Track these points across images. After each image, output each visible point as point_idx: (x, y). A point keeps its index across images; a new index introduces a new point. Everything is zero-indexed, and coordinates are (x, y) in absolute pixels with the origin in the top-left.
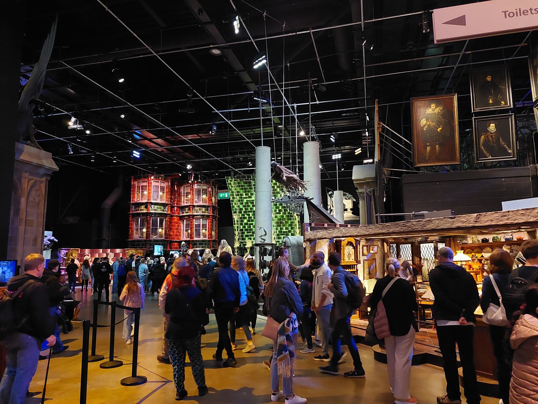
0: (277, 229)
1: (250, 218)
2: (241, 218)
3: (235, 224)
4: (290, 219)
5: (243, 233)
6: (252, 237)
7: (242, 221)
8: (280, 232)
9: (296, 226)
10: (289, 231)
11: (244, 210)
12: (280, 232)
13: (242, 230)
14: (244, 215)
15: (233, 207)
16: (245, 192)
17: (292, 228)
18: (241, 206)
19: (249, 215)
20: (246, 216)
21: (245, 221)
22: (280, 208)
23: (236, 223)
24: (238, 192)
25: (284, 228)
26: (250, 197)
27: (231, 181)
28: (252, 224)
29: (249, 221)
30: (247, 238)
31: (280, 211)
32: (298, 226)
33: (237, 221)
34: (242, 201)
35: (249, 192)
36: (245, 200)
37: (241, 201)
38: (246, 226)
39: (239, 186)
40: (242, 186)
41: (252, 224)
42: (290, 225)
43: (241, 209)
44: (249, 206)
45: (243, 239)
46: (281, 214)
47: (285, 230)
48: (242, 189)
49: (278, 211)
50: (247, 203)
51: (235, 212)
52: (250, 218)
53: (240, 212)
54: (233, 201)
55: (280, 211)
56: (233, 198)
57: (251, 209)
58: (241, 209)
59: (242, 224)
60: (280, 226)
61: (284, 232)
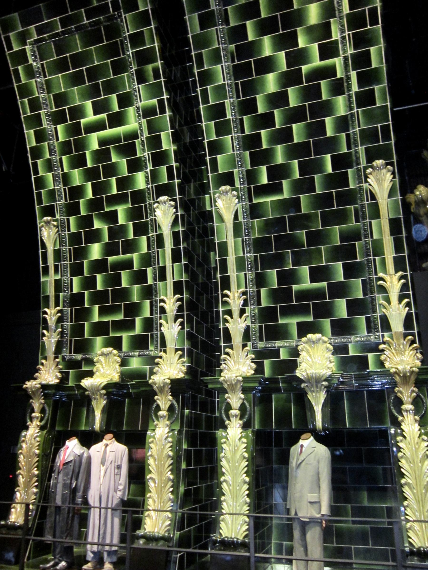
0: (260, 281)
1: (116, 232)
2: (75, 238)
3: (46, 271)
4: (341, 217)
5: (82, 314)
6: (125, 336)
7: (80, 253)
8: (274, 295)
9: (378, 250)
10: (338, 290)
11: (90, 194)
12: (281, 295)
13: (76, 300)
14: (87, 222)
15: (41, 182)
16: (94, 92)
17: (351, 271)
18: (77, 177)
19: (112, 217)
20: (97, 224)
22: (280, 158)
23: (51, 262)
24: (60, 99)
25: (305, 270)
26: (117, 120)
27: (23, 38)
28: (128, 265)
29: (110, 249)
30: (99, 340)
31: (278, 173)
32: (389, 253)
33: (58, 254)
34: (81, 145)
35: (110, 87)
36: (94, 141)
37: (74, 149)
38: (99, 278)
39: (61, 66)
40: (78, 60)
41: (128, 265)
42: (337, 254)
43: (76, 192)
44: (111, 170)
45: (83, 346)
46: (286, 195)
47: (307, 284)
48: (77, 79)
49: (264, 180)
50: (102, 155)
51: (49, 211)
52: (116, 232)
53: (72, 209)
54: (37, 153)
56: (41, 136)
57: (123, 183)
58: (76, 192)
59: (77, 270)
60: (277, 261)
61: (304, 295)
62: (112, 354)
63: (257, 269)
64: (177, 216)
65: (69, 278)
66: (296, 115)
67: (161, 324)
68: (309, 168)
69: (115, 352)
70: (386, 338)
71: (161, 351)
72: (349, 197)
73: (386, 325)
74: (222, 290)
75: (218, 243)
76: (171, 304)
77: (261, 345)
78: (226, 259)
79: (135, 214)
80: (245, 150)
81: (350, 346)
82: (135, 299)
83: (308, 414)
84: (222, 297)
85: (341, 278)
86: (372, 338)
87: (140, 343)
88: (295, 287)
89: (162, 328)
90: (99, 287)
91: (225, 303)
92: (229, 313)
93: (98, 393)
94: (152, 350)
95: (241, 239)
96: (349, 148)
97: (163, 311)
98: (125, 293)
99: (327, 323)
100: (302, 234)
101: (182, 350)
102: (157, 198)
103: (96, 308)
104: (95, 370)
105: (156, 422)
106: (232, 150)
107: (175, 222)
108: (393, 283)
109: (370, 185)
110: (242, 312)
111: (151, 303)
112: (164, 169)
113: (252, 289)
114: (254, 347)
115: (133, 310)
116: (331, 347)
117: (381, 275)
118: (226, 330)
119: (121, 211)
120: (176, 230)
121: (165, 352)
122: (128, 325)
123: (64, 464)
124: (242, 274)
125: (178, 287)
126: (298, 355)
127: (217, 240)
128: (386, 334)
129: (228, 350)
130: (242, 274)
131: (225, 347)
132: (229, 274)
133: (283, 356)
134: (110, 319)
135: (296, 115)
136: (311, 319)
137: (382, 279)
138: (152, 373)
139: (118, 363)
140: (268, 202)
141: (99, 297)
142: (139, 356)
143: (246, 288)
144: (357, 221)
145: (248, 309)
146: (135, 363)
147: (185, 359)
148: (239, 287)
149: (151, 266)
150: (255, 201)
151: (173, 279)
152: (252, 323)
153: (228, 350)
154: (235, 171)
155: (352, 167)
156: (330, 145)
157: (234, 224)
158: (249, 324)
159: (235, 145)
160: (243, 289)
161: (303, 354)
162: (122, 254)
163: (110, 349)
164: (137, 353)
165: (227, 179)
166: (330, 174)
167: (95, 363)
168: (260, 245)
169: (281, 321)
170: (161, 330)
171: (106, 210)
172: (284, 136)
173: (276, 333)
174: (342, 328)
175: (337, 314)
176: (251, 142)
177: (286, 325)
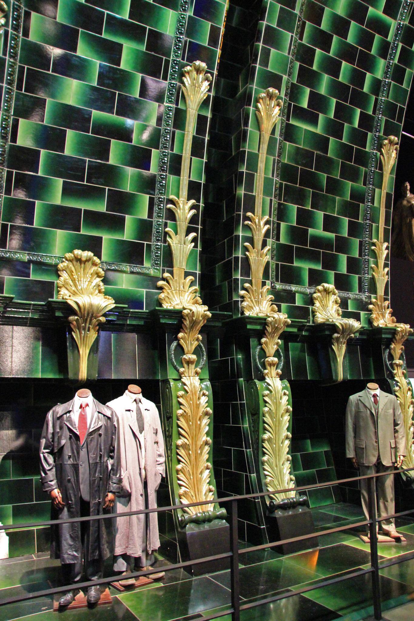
0: (282, 214)
4: (353, 175)
6: (107, 238)
8: (293, 232)
17: (354, 229)
19: (112, 52)
20: (83, 51)
21: (71, 92)
25: (320, 215)
29: (100, 98)
30: (60, 236)
38: (71, 135)
46: (319, 130)
55: (317, 101)
61: (317, 241)
62: (90, 263)
63: (280, 199)
64: (209, 97)
65: (12, 117)
66: (348, 53)
67: (166, 234)
68: (343, 113)
69: (96, 259)
70: (374, 300)
71: (163, 272)
72: (362, 158)
73: (373, 289)
74: (245, 211)
75: (248, 152)
76: (185, 210)
77: (279, 286)
78: (253, 175)
79: (153, 65)
80: (297, 60)
81: (349, 301)
82: (128, 187)
83: (332, 364)
84: (244, 221)
85: (346, 235)
86: (363, 297)
87: (132, 253)
88: (311, 231)
89: (168, 239)
90: (68, 151)
91: (247, 228)
92: (251, 240)
93: (94, 321)
94: (148, 267)
95: (272, 158)
96: (374, 112)
97: (171, 216)
98: (110, 174)
99: (331, 274)
100: (324, 176)
101: (194, 274)
102: (191, 60)
103: (59, 183)
104: (60, 282)
105: (182, 370)
106: (287, 52)
107: (205, 103)
108: (383, 250)
109: (382, 154)
110: (264, 244)
111: (151, 201)
112: (207, 25)
113: (274, 219)
114: (272, 287)
115: (122, 202)
116: (339, 301)
117: (375, 240)
118: (246, 260)
119: (130, 51)
120: (203, 113)
121: (172, 273)
122: (117, 224)
123: (91, 434)
124: (268, 199)
125: (194, 190)
126: (313, 304)
127: (248, 149)
128: (372, 296)
129: (247, 285)
130: (268, 199)
131: (244, 282)
132: (254, 194)
133: (299, 302)
134: (83, 206)
135: (348, 53)
136: (319, 267)
137: (374, 244)
138: (242, 301)
139: (99, 276)
140: (302, 128)
141: (62, 167)
142: (132, 273)
143: (270, 216)
144: (365, 184)
145: (270, 241)
146: (125, 282)
147: (197, 287)
148: (263, 214)
149: (158, 148)
150: (291, 122)
151: (189, 177)
152: (272, 258)
153: (247, 285)
154: (285, 77)
155: (371, 132)
156: (360, 100)
157: (270, 138)
158: (270, 260)
159: (292, 48)
160: (266, 217)
161: (317, 304)
162: (117, 114)
163: (90, 254)
164: (126, 267)
165: (273, 80)
166: (355, 128)
167: (60, 270)
168: (286, 172)
169: (296, 264)
170: (165, 241)
171: (104, 36)
172: (332, 67)
173: (289, 275)
174: (342, 283)
175: (340, 268)
176: (305, 55)
177: (299, 269)
